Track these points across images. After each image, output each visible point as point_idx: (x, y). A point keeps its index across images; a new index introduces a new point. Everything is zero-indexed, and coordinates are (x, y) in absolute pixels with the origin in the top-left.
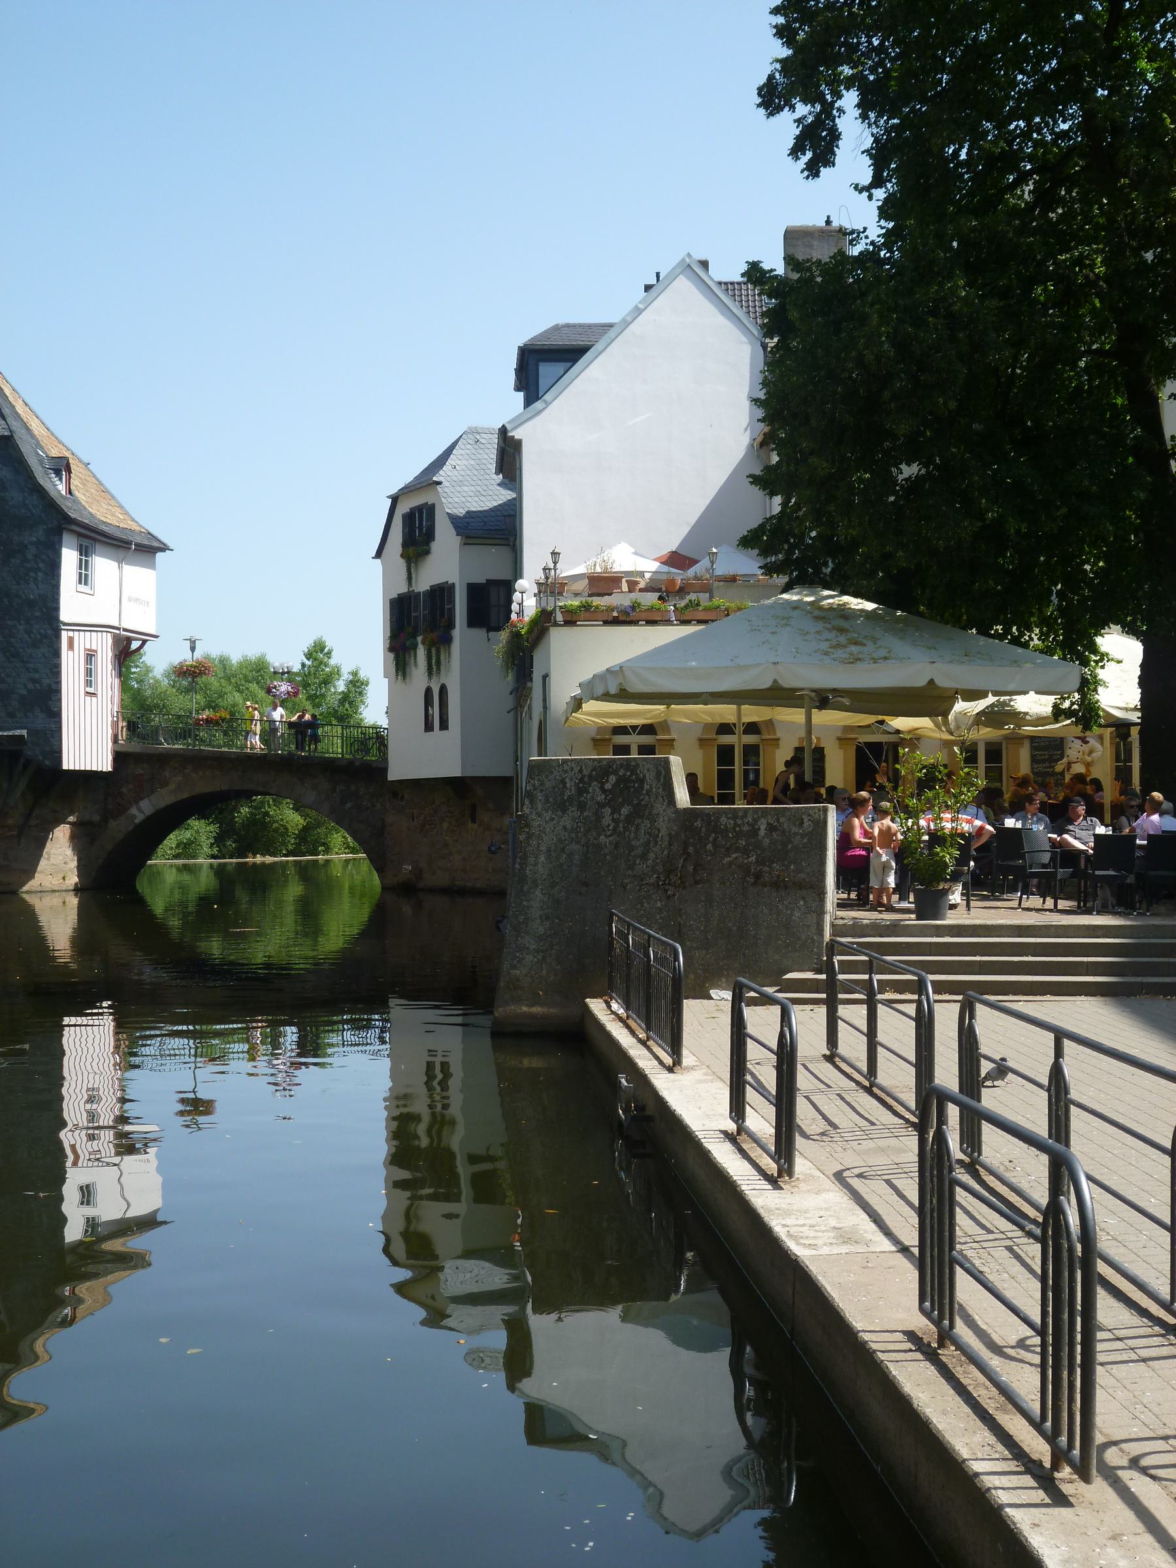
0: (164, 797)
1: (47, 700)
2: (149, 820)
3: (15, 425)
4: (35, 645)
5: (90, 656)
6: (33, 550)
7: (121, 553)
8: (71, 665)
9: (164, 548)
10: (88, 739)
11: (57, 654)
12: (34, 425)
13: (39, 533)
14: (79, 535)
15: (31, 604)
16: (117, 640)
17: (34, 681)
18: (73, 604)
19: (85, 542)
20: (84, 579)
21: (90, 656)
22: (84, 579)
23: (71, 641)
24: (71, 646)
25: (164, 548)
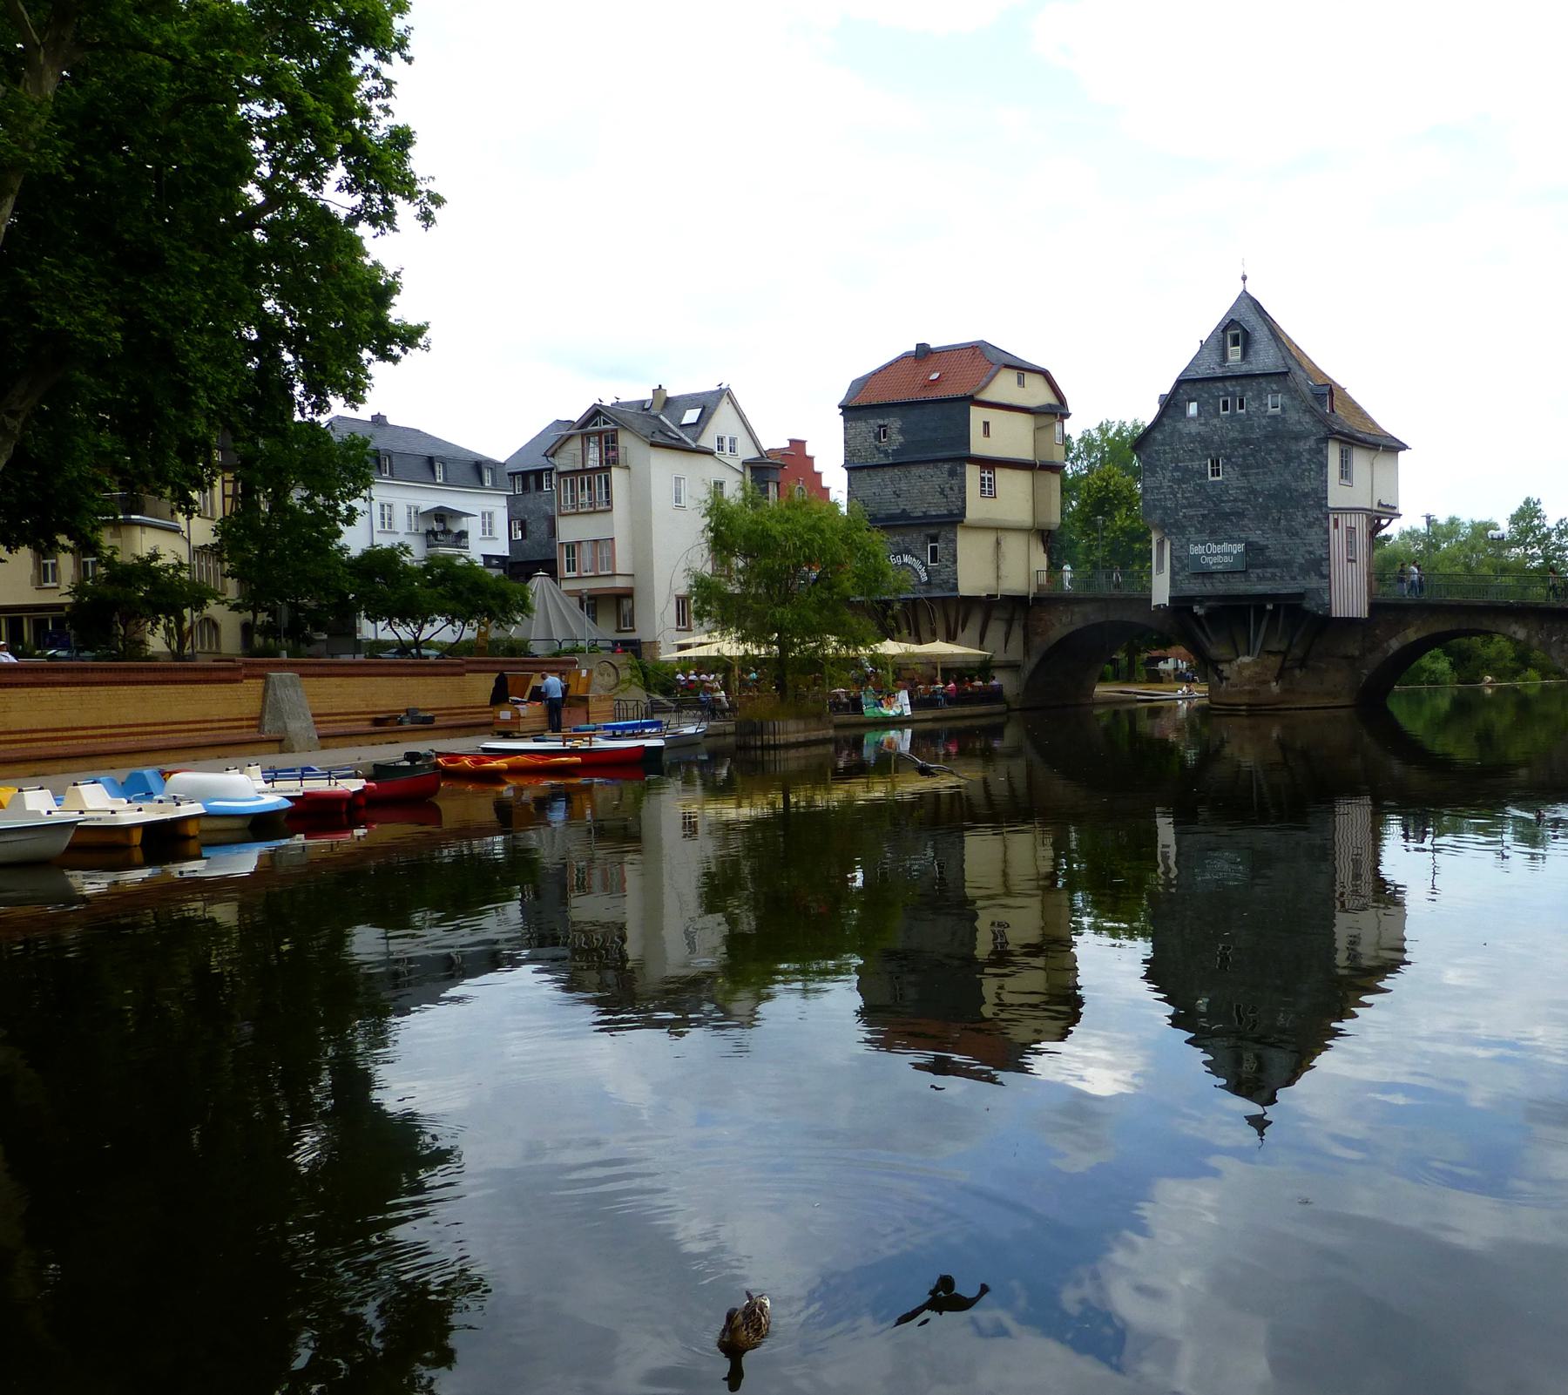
0: (1412, 635)
1: (1319, 565)
2: (1398, 653)
3: (1291, 363)
4: (1310, 525)
5: (1351, 531)
6: (1306, 455)
7: (1373, 454)
8: (1338, 538)
9: (1404, 447)
10: (1349, 595)
11: (1327, 531)
12: (1304, 363)
13: (1311, 443)
14: (1341, 442)
15: (1306, 495)
16: (1370, 520)
17: (1310, 553)
18: (1337, 495)
19: (1346, 447)
20: (1345, 474)
21: (1351, 531)
22: (1345, 474)
23: (1336, 521)
24: (1336, 526)
25: (1404, 447)
